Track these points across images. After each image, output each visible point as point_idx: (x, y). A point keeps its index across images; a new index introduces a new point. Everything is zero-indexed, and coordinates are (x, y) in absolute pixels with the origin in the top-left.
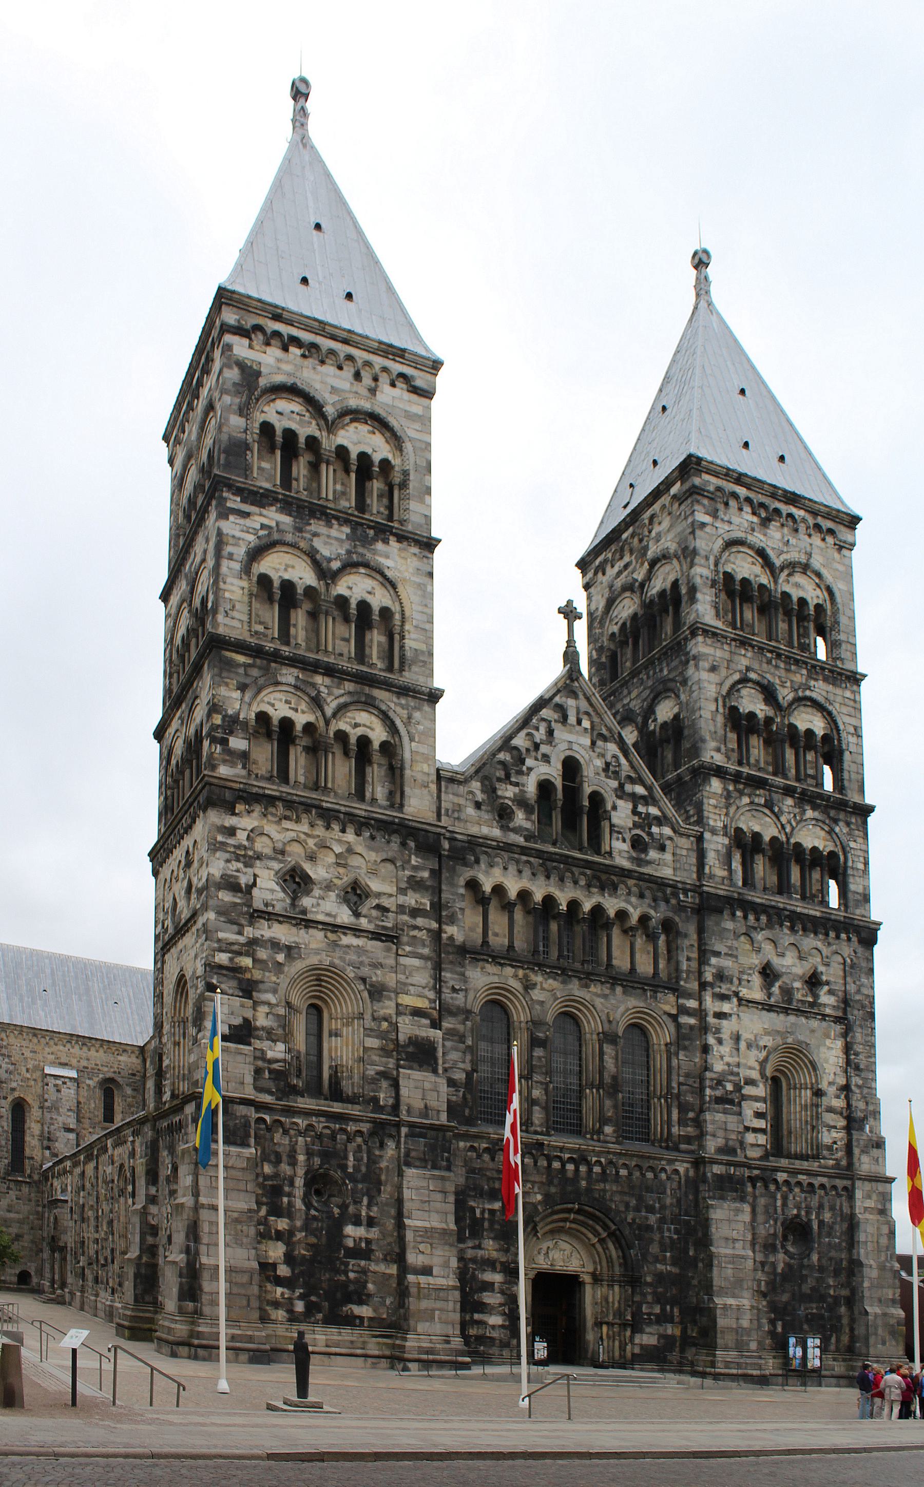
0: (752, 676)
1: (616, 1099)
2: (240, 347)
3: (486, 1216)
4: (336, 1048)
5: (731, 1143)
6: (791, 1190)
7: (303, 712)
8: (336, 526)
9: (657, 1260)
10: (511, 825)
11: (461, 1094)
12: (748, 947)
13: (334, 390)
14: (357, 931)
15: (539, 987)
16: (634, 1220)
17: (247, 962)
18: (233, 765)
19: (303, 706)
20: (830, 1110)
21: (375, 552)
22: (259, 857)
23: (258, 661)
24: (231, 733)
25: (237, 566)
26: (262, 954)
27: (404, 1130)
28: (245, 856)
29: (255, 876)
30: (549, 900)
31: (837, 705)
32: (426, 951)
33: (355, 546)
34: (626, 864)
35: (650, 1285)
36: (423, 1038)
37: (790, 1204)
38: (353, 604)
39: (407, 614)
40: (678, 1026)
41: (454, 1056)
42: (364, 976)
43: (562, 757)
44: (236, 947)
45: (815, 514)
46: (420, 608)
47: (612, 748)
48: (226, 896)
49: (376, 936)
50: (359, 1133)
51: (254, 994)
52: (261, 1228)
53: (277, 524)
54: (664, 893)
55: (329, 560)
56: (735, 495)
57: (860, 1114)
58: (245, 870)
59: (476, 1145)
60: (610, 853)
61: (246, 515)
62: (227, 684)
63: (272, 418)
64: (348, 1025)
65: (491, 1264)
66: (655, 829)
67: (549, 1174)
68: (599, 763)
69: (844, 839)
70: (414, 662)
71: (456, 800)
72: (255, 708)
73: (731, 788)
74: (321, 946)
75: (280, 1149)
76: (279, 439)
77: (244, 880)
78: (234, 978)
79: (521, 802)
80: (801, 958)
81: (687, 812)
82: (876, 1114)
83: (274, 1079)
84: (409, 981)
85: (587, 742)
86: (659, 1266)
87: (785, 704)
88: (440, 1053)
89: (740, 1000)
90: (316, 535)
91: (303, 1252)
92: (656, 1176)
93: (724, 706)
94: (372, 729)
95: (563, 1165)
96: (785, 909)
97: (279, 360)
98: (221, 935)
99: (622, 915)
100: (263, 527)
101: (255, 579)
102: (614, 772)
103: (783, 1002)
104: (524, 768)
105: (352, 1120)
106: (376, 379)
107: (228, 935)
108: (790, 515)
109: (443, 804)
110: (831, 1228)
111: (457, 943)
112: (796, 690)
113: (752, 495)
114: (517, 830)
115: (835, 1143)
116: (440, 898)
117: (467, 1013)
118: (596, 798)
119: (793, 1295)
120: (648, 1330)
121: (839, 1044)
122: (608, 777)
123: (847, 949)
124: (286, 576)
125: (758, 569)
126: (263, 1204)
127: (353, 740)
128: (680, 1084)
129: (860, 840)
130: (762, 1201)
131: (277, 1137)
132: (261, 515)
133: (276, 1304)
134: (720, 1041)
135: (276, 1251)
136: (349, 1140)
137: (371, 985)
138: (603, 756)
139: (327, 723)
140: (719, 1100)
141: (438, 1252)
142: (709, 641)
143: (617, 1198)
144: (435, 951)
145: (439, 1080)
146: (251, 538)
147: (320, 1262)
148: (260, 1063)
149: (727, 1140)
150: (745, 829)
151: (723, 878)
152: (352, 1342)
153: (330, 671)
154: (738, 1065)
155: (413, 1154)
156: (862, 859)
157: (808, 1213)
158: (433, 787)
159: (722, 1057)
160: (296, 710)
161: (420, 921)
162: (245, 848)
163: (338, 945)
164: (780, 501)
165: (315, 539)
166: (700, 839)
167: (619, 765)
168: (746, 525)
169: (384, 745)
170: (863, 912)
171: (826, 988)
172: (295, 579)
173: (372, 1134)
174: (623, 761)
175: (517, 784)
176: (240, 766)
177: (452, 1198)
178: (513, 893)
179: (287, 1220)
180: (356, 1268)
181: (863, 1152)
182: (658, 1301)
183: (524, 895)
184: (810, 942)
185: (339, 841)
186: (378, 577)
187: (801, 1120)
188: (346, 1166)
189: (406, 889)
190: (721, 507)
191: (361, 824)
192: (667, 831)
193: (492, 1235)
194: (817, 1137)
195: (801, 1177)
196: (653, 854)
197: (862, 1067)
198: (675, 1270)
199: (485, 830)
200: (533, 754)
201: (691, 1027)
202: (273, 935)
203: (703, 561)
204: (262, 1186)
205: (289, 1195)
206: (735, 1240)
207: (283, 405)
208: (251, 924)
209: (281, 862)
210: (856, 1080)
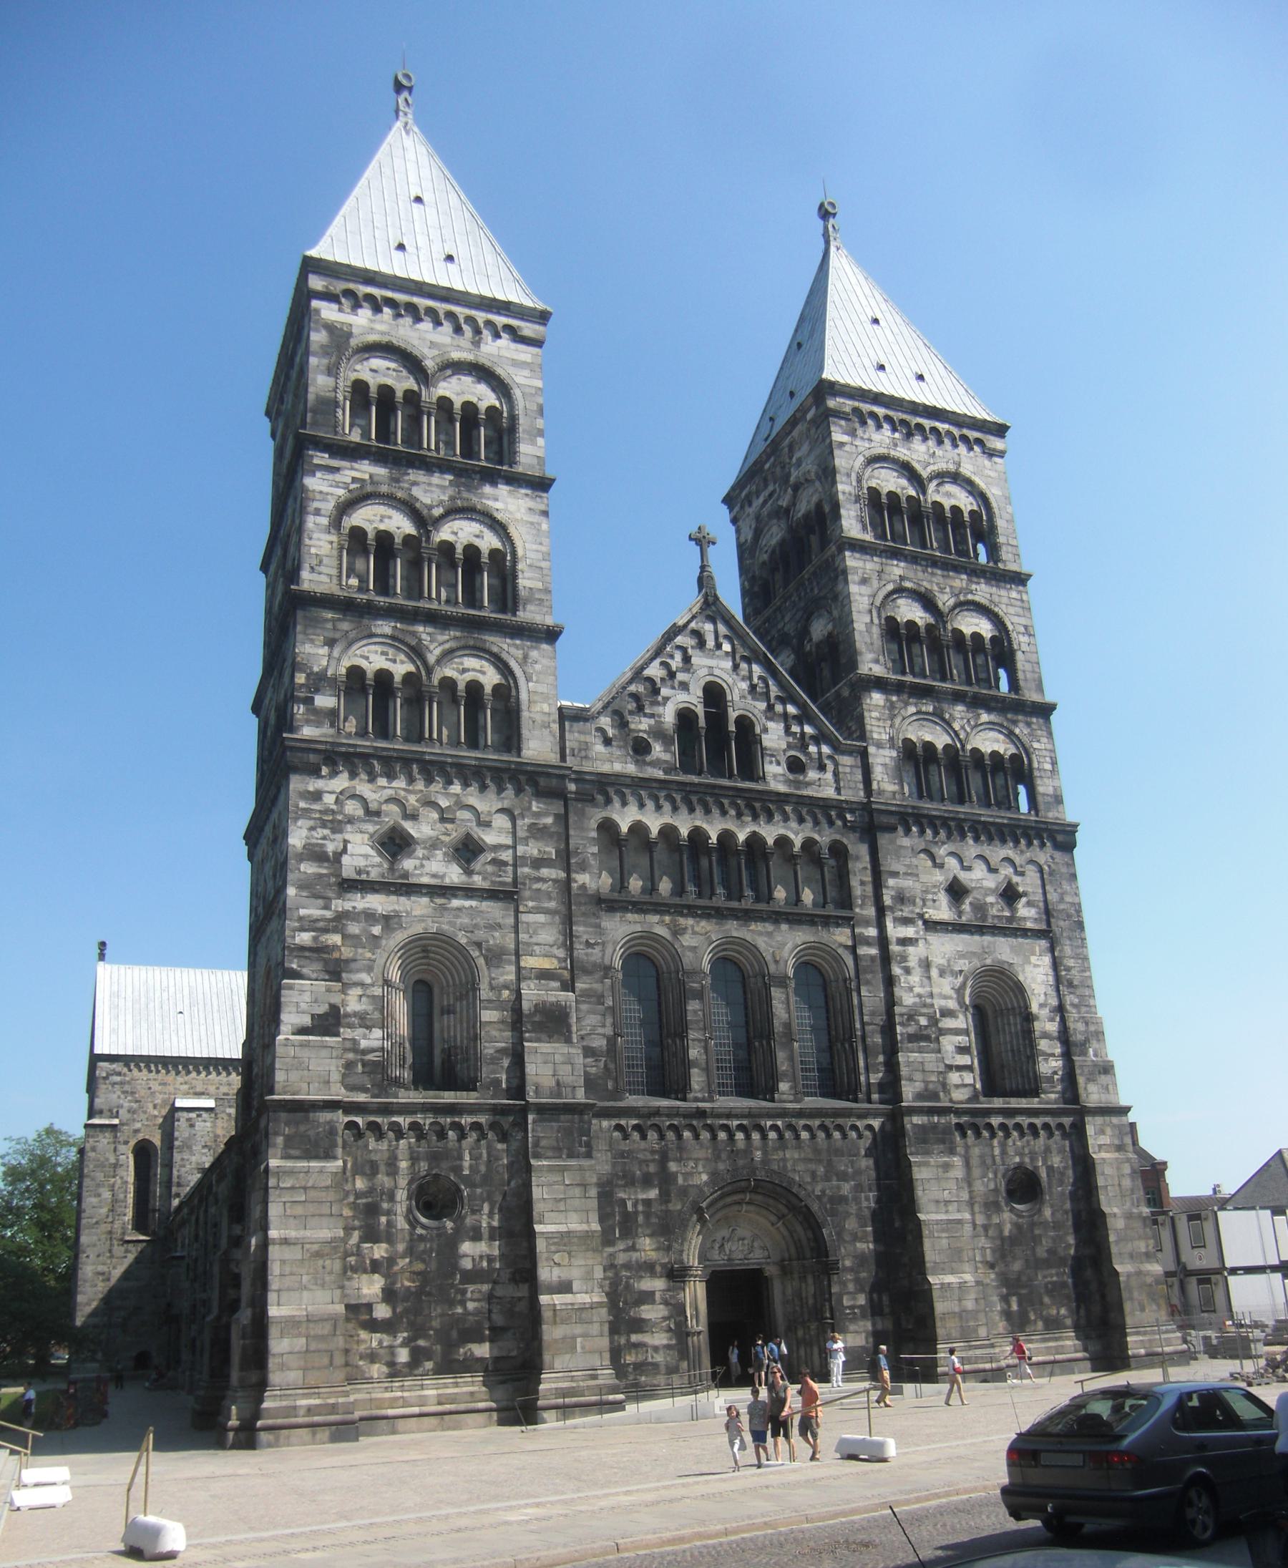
0: (908, 584)
1: (792, 1050)
2: (328, 311)
3: (640, 1208)
5: (931, 1086)
6: (1008, 1135)
7: (402, 662)
9: (855, 1238)
10: (648, 759)
11: (602, 1064)
12: (929, 863)
13: (433, 345)
14: (469, 892)
16: (823, 1191)
17: (336, 939)
18: (318, 724)
19: (402, 657)
20: (1046, 1035)
21: (482, 496)
22: (350, 820)
24: (317, 691)
26: (354, 928)
29: (346, 842)
30: (697, 836)
31: (1003, 607)
32: (552, 904)
34: (782, 788)
35: (851, 1270)
36: (552, 1004)
37: (1011, 1151)
38: (459, 549)
39: (520, 552)
40: (856, 958)
41: (592, 1020)
43: (702, 683)
44: (321, 924)
46: (535, 547)
47: (757, 669)
48: (309, 868)
49: (491, 895)
50: (476, 1126)
51: (344, 975)
53: (371, 476)
55: (430, 508)
56: (873, 415)
57: (1080, 1037)
59: (623, 1122)
60: (764, 777)
61: (337, 470)
62: (312, 641)
63: (366, 376)
64: (461, 998)
65: (649, 1268)
66: (813, 749)
67: (715, 1148)
68: (744, 685)
69: (1025, 739)
71: (582, 738)
72: (346, 663)
74: (424, 911)
75: (374, 1157)
77: (330, 848)
78: (318, 960)
79: (658, 733)
80: (992, 870)
82: (1099, 1035)
83: (369, 1073)
84: (534, 940)
85: (728, 664)
86: (858, 1245)
87: (945, 610)
88: (573, 1020)
89: (926, 922)
90: (415, 483)
91: (407, 1284)
92: (845, 1136)
93: (879, 617)
94: (483, 673)
95: (731, 1136)
96: (965, 820)
98: (302, 912)
99: (783, 842)
100: (354, 480)
102: (761, 694)
103: (976, 919)
106: (477, 332)
107: (312, 911)
108: (933, 430)
109: (568, 744)
110: (1062, 1174)
111: (590, 892)
113: (891, 413)
114: (656, 764)
115: (1055, 1073)
116: (567, 844)
117: (607, 970)
118: (745, 724)
119: (1027, 1261)
120: (852, 1327)
121: (1047, 960)
122: (753, 699)
124: (382, 527)
125: (904, 482)
126: (354, 1229)
127: (461, 686)
128: (863, 1024)
129: (1044, 740)
130: (976, 1151)
132: (352, 469)
133: (372, 1357)
135: (371, 1287)
136: (462, 1136)
137: (488, 950)
138: (750, 678)
139: (429, 671)
140: (913, 1038)
143: (800, 1167)
144: (563, 903)
145: (572, 1051)
146: (341, 492)
147: (429, 1294)
148: (351, 1056)
149: (926, 1082)
151: (894, 793)
152: (472, 1394)
153: (433, 619)
154: (931, 995)
155: (543, 1143)
157: (1033, 1159)
158: (556, 727)
159: (911, 989)
160: (394, 661)
161: (545, 872)
162: (333, 812)
163: (446, 909)
164: (921, 416)
166: (864, 755)
167: (767, 686)
169: (496, 688)
170: (1056, 815)
171: (1024, 900)
173: (493, 1126)
175: (652, 716)
177: (593, 1192)
178: (654, 831)
179: (384, 1245)
180: (476, 1296)
181: (1089, 1080)
182: (862, 1290)
184: (998, 852)
185: (447, 795)
186: (487, 520)
187: (1012, 1051)
188: (460, 1168)
189: (526, 839)
190: (857, 425)
191: (473, 775)
192: (826, 749)
194: (1035, 1072)
196: (812, 775)
199: (618, 767)
200: (669, 683)
201: (872, 958)
202: (367, 905)
203: (844, 479)
204: (354, 1206)
205: (389, 1213)
206: (947, 1202)
207: (377, 363)
209: (376, 823)
210: (1070, 999)
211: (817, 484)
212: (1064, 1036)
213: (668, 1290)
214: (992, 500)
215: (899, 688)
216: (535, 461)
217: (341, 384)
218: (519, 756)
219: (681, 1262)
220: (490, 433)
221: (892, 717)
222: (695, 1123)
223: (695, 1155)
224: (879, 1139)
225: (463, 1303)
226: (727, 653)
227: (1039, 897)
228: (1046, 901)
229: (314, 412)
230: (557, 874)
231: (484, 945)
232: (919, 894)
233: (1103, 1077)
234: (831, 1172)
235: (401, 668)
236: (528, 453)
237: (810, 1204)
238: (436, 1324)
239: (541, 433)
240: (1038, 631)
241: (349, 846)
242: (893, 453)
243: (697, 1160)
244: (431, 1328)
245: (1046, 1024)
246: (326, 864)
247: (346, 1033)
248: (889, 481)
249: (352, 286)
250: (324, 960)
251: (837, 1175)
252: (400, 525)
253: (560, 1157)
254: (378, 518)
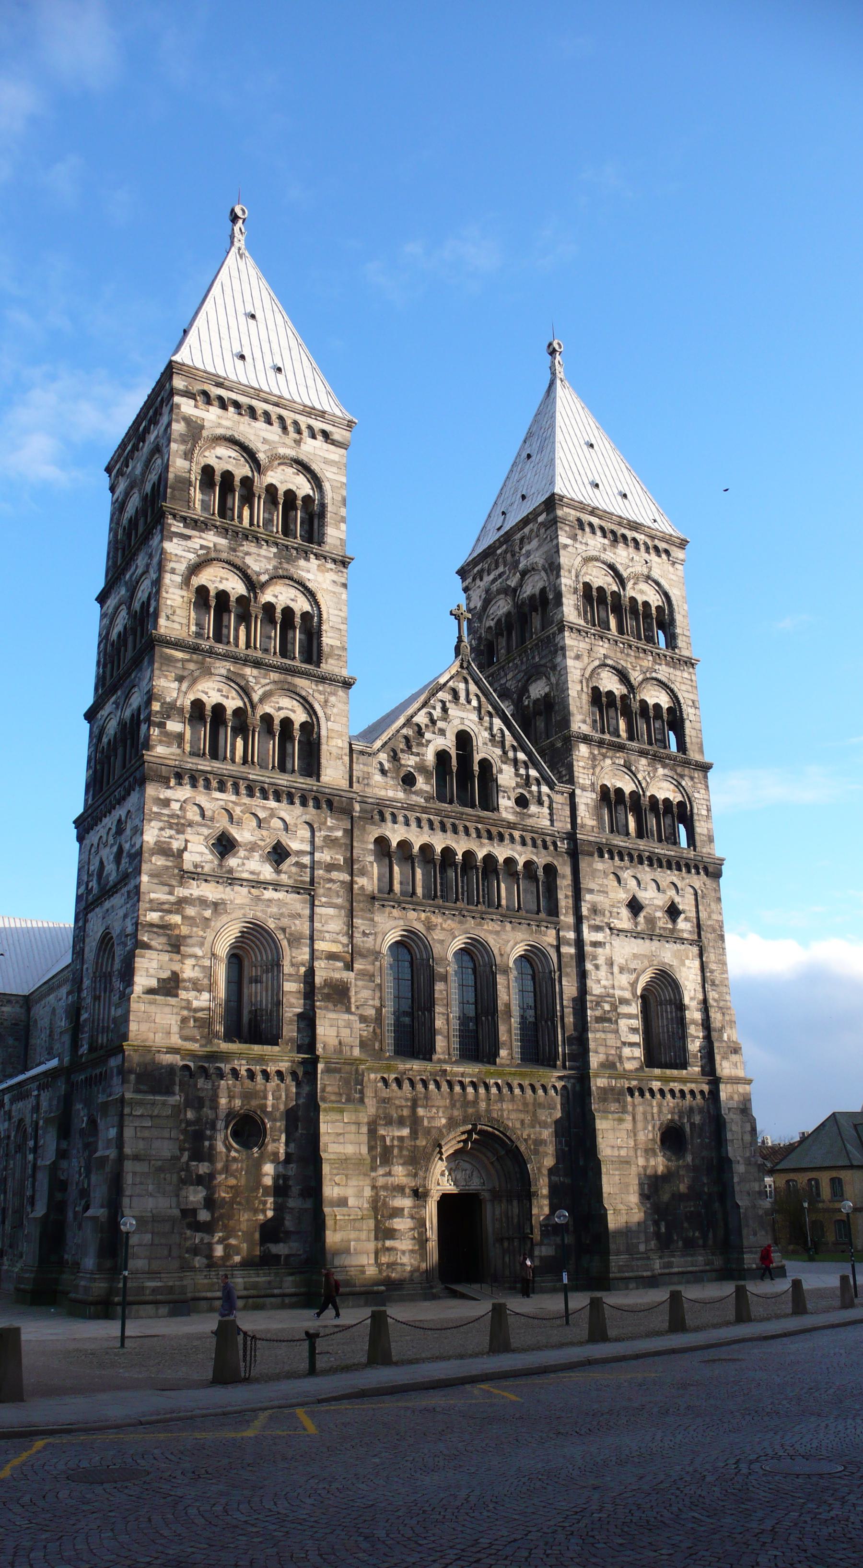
0: (609, 662)
2: (186, 406)
3: (396, 1143)
4: (256, 993)
5: (611, 1058)
7: (233, 699)
8: (265, 547)
10: (413, 789)
11: (371, 1029)
12: (616, 884)
13: (265, 441)
14: (277, 886)
15: (439, 928)
16: (529, 1136)
17: (176, 919)
18: (169, 745)
19: (234, 694)
20: (693, 1022)
21: (298, 568)
22: (190, 824)
23: (195, 656)
24: (168, 717)
25: (178, 579)
26: (191, 911)
27: (320, 1066)
28: (177, 824)
30: (448, 852)
32: (339, 901)
33: (280, 563)
34: (511, 817)
36: (337, 980)
37: (665, 1110)
39: (325, 616)
41: (366, 994)
42: (285, 926)
44: (166, 907)
45: (652, 538)
46: (336, 612)
47: (497, 723)
48: (159, 861)
49: (297, 890)
50: (279, 1073)
51: (182, 948)
52: (183, 1173)
53: (215, 545)
54: (544, 842)
58: (177, 836)
59: (385, 1076)
61: (189, 538)
62: (166, 677)
63: (212, 462)
64: (267, 972)
65: (400, 1189)
66: (534, 788)
67: (452, 1099)
69: (689, 790)
70: (330, 655)
71: (366, 769)
72: (192, 697)
73: (596, 752)
75: (202, 1094)
76: (218, 478)
81: (560, 772)
83: (199, 1027)
84: (325, 928)
85: (474, 717)
87: (635, 683)
88: (352, 993)
91: (223, 1195)
93: (588, 686)
94: (294, 711)
97: (220, 417)
98: (153, 896)
99: (510, 861)
100: (202, 547)
101: (193, 589)
102: (498, 742)
104: (424, 741)
105: (272, 1060)
107: (159, 895)
108: (634, 540)
109: (355, 773)
111: (367, 893)
112: (645, 673)
113: (603, 524)
118: (485, 764)
121: (697, 963)
122: (493, 746)
123: (698, 881)
124: (221, 587)
125: (610, 579)
126: (185, 1150)
129: (702, 791)
130: (640, 1109)
131: (201, 1082)
132: (201, 538)
133: (195, 1251)
134: (597, 967)
137: (291, 934)
138: (491, 729)
139: (253, 707)
140: (599, 1020)
141: (353, 1182)
142: (573, 635)
145: (352, 1017)
146: (192, 556)
148: (185, 1013)
149: (607, 1055)
150: (609, 786)
151: (593, 827)
153: (257, 664)
154: (613, 987)
155: (329, 1089)
156: (705, 807)
157: (680, 1117)
159: (599, 981)
160: (227, 697)
161: (335, 875)
162: (178, 817)
163: (260, 900)
165: (247, 557)
166: (572, 795)
167: (503, 736)
168: (599, 546)
169: (303, 725)
170: (709, 851)
171: (682, 916)
172: (228, 590)
174: (507, 733)
175: (418, 754)
176: (175, 746)
177: (364, 1129)
179: (206, 1164)
183: (426, 849)
184: (667, 877)
185: (264, 808)
188: (265, 1106)
189: (322, 847)
190: (579, 532)
192: (545, 789)
193: (401, 1161)
195: (672, 1085)
196: (533, 809)
197: (717, 982)
198: (568, 1181)
199: (391, 794)
200: (431, 729)
201: (571, 955)
202: (201, 893)
203: (567, 574)
208: (181, 884)
209: (209, 827)
210: (712, 995)
211: (543, 574)
212: (706, 1024)
213: (414, 1207)
214: (673, 599)
215: (601, 743)
216: (338, 543)
217: (194, 468)
218: (318, 781)
219: (424, 1186)
220: (304, 515)
221: (594, 767)
222: (438, 1078)
223: (437, 1104)
224: (571, 1096)
225: (264, 1211)
226: (474, 707)
227: (694, 914)
228: (698, 918)
229: (173, 489)
230: (345, 877)
231: (288, 930)
232: (607, 907)
233: (733, 1055)
234: (535, 1121)
235: (232, 703)
236: (334, 534)
237: (519, 1144)
238: (244, 1226)
239: (343, 520)
240: (701, 704)
241: (189, 844)
242: (603, 555)
243: (438, 1107)
244: (240, 1230)
245: (694, 1014)
246: (171, 859)
247: (183, 994)
248: (600, 578)
249: (206, 387)
250: (168, 935)
251: (539, 1124)
252: (236, 587)
253: (339, 1102)
254: (219, 579)
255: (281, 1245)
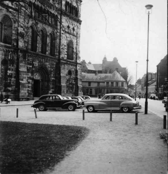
40: (57, 35)
50: (11, 51)
92: (53, 62)
123: (78, 24)
128: (57, 45)
171: (75, 31)
198: (54, 79)
210: (77, 47)
255: (10, 88)
